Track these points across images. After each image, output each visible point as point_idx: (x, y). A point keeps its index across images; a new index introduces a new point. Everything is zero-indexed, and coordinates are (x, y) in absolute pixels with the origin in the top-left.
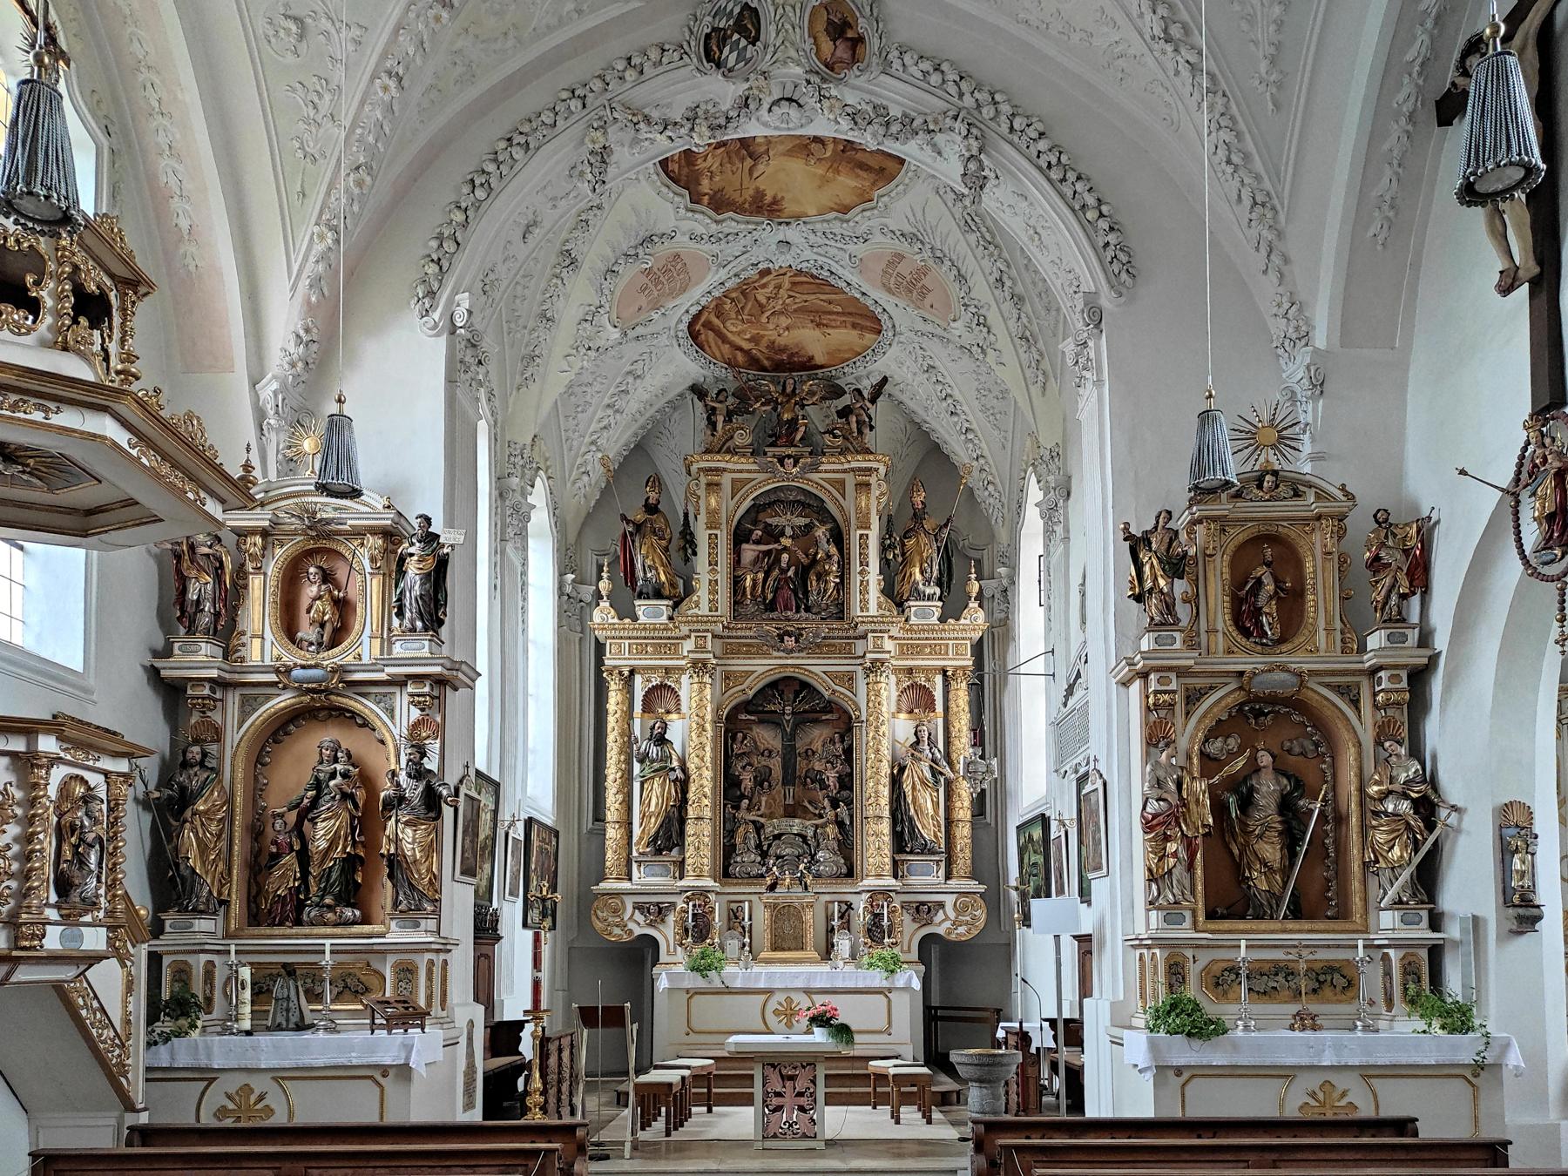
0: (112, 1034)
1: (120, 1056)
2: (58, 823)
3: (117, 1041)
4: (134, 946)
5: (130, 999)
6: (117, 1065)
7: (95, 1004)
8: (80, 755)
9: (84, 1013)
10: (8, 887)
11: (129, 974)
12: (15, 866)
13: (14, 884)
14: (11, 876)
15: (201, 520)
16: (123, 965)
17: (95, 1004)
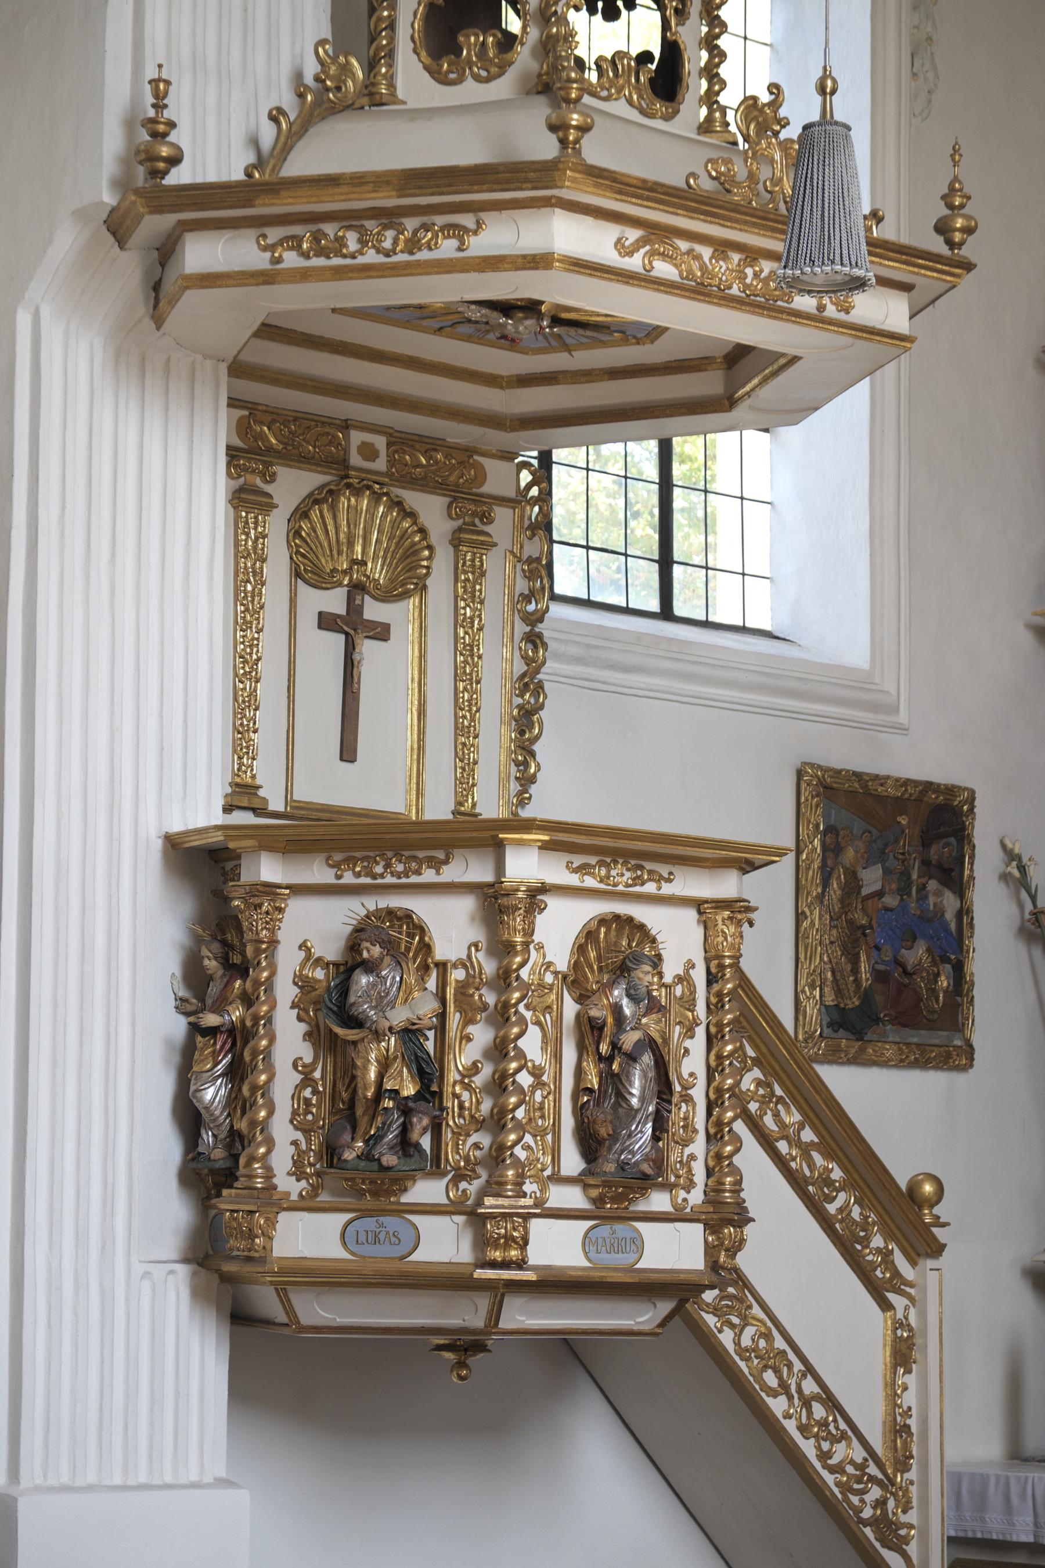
0: (859, 1454)
1: (881, 1503)
2: (578, 1017)
3: (873, 1470)
4: (913, 1263)
5: (911, 1380)
6: (872, 1522)
7: (809, 1386)
8: (622, 877)
9: (778, 1405)
10: (476, 1146)
11: (898, 1325)
12: (486, 1106)
13: (484, 1139)
14: (479, 1124)
15: (846, 340)
16: (885, 1306)
17: (809, 1386)
